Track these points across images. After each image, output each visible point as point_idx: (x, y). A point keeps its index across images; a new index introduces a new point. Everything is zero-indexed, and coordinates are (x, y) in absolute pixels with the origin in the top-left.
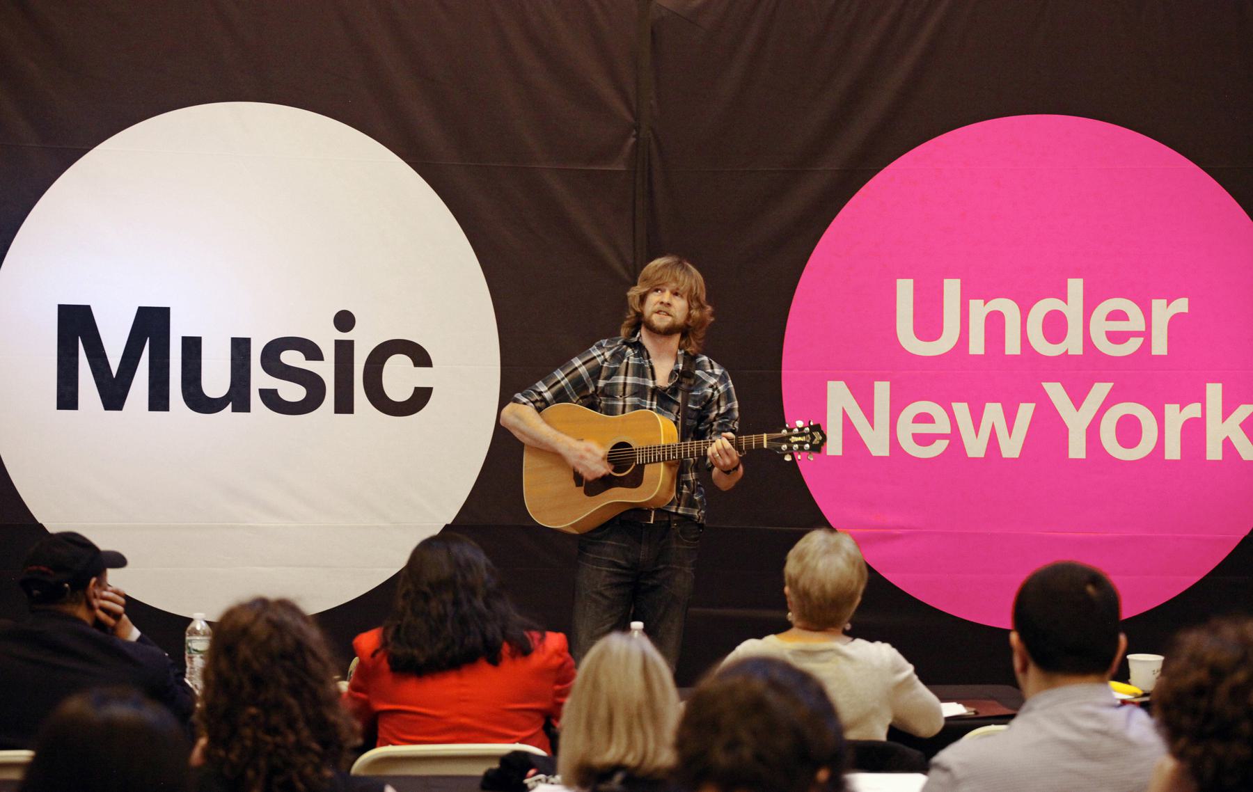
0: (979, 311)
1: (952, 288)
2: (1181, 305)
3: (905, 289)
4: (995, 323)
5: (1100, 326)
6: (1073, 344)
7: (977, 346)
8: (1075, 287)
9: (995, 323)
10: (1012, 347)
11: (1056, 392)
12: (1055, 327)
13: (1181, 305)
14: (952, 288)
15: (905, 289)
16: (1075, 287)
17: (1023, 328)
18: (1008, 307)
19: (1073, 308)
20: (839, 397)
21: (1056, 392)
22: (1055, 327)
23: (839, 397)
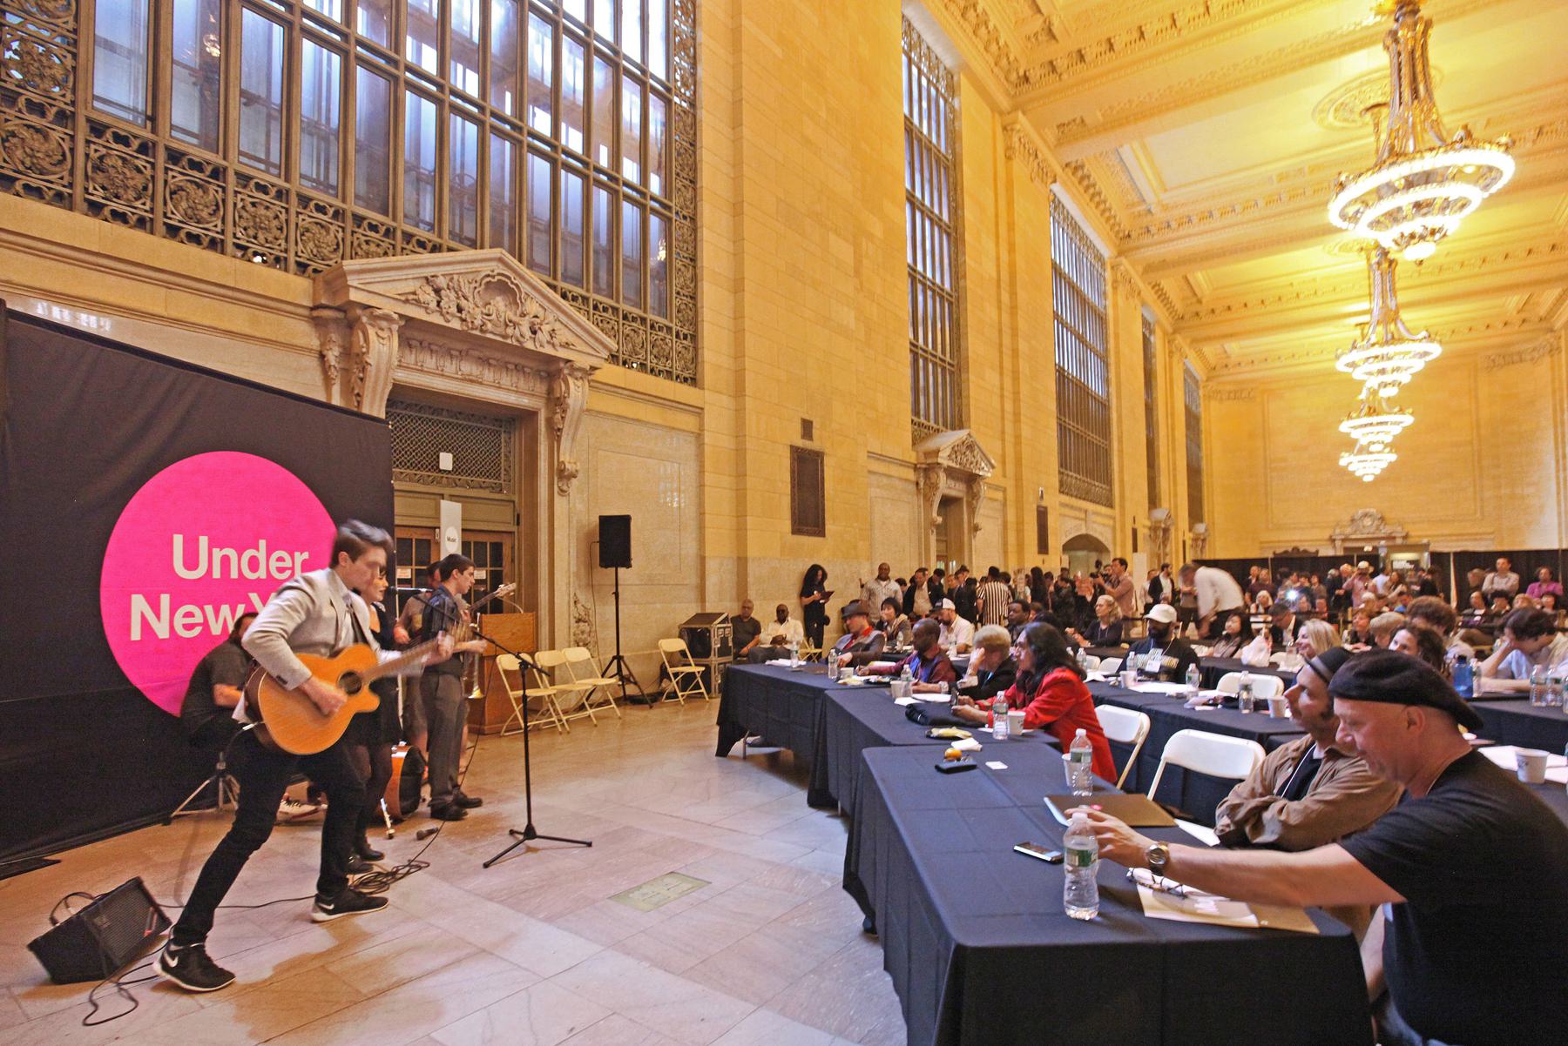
0: (218, 554)
1: (204, 541)
2: (306, 555)
3: (178, 540)
4: (225, 561)
5: (274, 564)
6: (262, 574)
7: (217, 574)
8: (262, 543)
9: (225, 561)
10: (234, 575)
11: (254, 597)
12: (254, 564)
13: (306, 555)
14: (204, 541)
15: (178, 540)
16: (262, 543)
17: (239, 566)
18: (231, 553)
19: (261, 554)
20: (139, 604)
21: (254, 597)
22: (254, 564)
23: (139, 604)
